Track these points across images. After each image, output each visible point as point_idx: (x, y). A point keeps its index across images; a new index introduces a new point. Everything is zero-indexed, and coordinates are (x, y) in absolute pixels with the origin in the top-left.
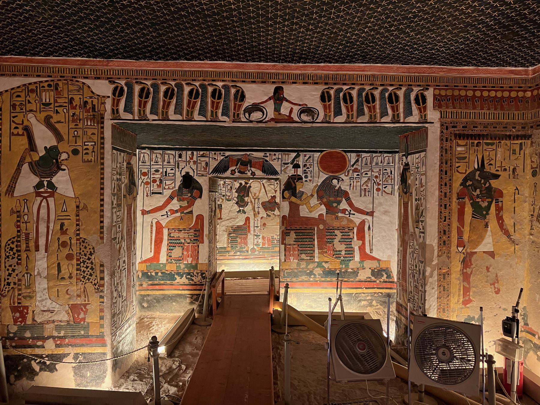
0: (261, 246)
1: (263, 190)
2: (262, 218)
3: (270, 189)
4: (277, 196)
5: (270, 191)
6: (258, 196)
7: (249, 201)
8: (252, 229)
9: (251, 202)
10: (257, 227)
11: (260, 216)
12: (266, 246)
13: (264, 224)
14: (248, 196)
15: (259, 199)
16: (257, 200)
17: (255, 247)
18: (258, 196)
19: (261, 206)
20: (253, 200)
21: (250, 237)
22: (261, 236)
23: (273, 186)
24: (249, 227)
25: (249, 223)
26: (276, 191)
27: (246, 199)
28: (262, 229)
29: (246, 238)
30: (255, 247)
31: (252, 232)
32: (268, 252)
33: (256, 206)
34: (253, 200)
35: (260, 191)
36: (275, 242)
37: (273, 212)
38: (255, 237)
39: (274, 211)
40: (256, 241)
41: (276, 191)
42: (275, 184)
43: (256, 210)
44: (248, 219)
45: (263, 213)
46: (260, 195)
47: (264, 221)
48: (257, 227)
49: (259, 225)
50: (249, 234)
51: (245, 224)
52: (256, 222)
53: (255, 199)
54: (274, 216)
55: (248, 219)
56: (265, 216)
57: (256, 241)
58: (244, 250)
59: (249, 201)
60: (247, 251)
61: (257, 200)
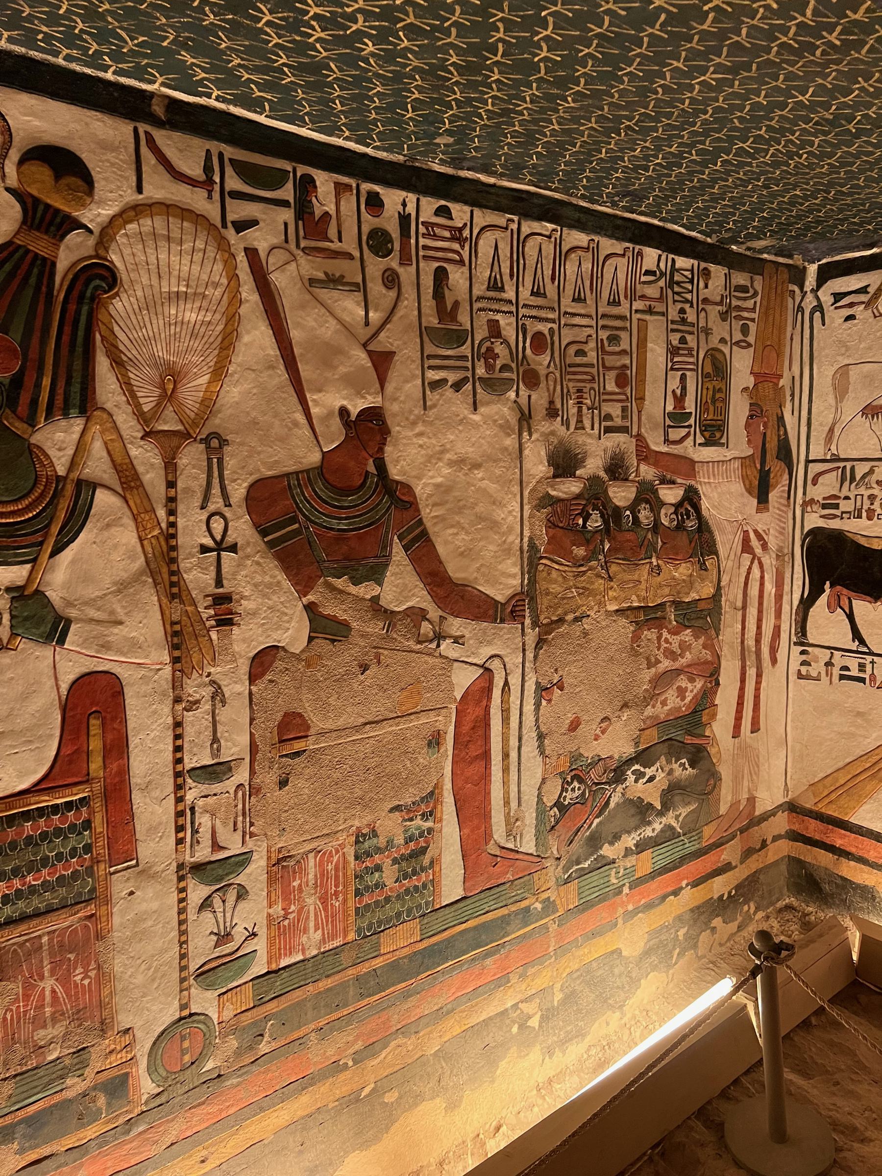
0: (259, 968)
1: (256, 337)
2: (263, 662)
3: (329, 330)
4: (392, 408)
5: (329, 354)
6: (208, 405)
7: (97, 465)
8: (152, 809)
9: (128, 480)
10: (214, 772)
11: (246, 639)
12: (312, 941)
13: (292, 727)
14: (81, 400)
15: (215, 445)
16: (191, 458)
17: (204, 1001)
18: (208, 405)
19: (242, 528)
20: (146, 458)
21: (143, 912)
22: (258, 865)
23: (351, 307)
24: (118, 793)
25: (118, 747)
26: (382, 362)
27: (58, 441)
28: (268, 778)
29: (86, 945)
30: (204, 1001)
31: (156, 845)
32: (333, 1000)
33: (193, 529)
34: (146, 458)
35: (227, 343)
36: (389, 875)
37: (367, 590)
38: (197, 892)
39: (376, 574)
40: (202, 928)
41: (382, 362)
42: (376, 288)
43: (197, 577)
44: (94, 704)
45: (272, 612)
46: (234, 393)
47: (282, 693)
48: (214, 772)
49: (236, 745)
50: (120, 886)
51: (63, 771)
52: (196, 723)
53: (170, 445)
54: (376, 628)
55: (94, 704)
56: (293, 633)
57: (202, 928)
58: (75, 1086)
59: (97, 465)
60: (117, 1086)
61: (191, 458)
